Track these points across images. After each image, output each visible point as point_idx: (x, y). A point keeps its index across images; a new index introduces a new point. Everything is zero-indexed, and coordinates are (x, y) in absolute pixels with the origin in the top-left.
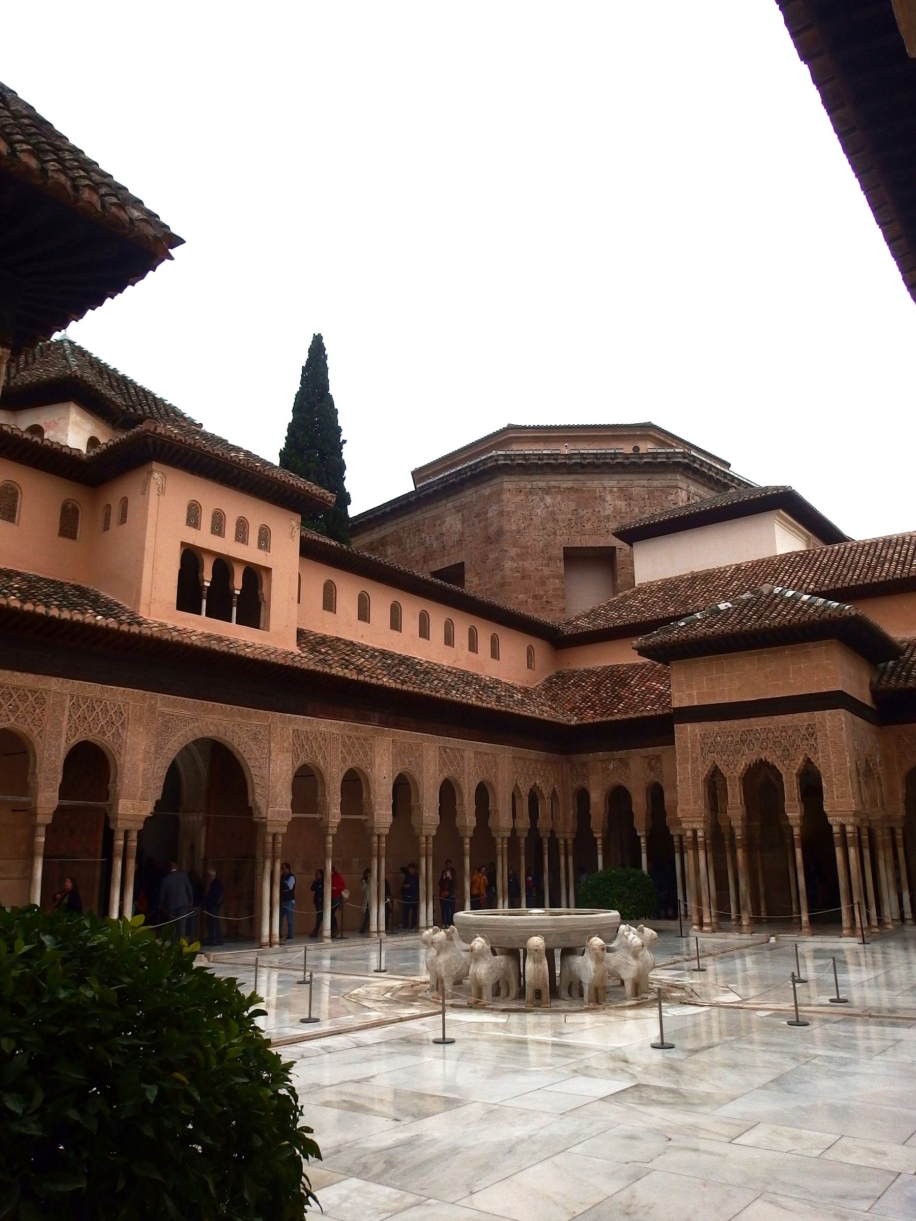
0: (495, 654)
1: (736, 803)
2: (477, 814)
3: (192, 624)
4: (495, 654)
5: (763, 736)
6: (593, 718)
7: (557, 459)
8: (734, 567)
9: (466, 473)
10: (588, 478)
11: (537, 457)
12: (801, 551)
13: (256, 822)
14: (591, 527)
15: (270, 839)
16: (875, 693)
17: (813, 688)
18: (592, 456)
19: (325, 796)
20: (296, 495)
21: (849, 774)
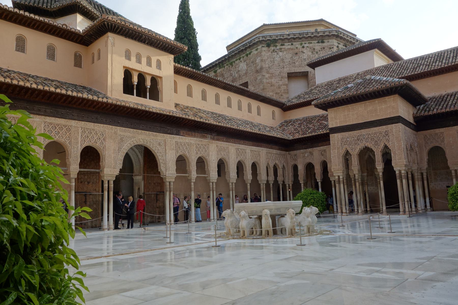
0: (259, 114)
1: (356, 165)
2: (253, 174)
3: (130, 99)
4: (259, 114)
5: (367, 137)
6: (298, 136)
7: (283, 37)
8: (356, 74)
9: (247, 45)
10: (296, 44)
11: (275, 36)
12: (385, 65)
13: (162, 178)
14: (298, 64)
15: (168, 184)
16: (415, 118)
17: (387, 116)
18: (298, 34)
19: (189, 167)
20: (170, 46)
21: (403, 150)
